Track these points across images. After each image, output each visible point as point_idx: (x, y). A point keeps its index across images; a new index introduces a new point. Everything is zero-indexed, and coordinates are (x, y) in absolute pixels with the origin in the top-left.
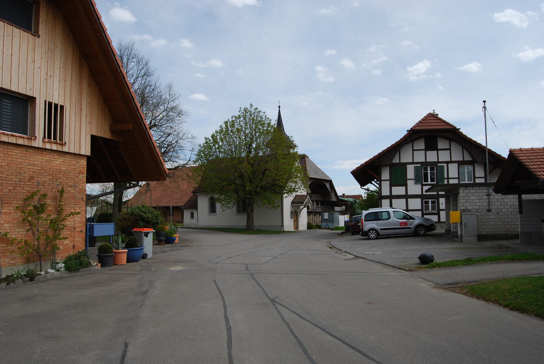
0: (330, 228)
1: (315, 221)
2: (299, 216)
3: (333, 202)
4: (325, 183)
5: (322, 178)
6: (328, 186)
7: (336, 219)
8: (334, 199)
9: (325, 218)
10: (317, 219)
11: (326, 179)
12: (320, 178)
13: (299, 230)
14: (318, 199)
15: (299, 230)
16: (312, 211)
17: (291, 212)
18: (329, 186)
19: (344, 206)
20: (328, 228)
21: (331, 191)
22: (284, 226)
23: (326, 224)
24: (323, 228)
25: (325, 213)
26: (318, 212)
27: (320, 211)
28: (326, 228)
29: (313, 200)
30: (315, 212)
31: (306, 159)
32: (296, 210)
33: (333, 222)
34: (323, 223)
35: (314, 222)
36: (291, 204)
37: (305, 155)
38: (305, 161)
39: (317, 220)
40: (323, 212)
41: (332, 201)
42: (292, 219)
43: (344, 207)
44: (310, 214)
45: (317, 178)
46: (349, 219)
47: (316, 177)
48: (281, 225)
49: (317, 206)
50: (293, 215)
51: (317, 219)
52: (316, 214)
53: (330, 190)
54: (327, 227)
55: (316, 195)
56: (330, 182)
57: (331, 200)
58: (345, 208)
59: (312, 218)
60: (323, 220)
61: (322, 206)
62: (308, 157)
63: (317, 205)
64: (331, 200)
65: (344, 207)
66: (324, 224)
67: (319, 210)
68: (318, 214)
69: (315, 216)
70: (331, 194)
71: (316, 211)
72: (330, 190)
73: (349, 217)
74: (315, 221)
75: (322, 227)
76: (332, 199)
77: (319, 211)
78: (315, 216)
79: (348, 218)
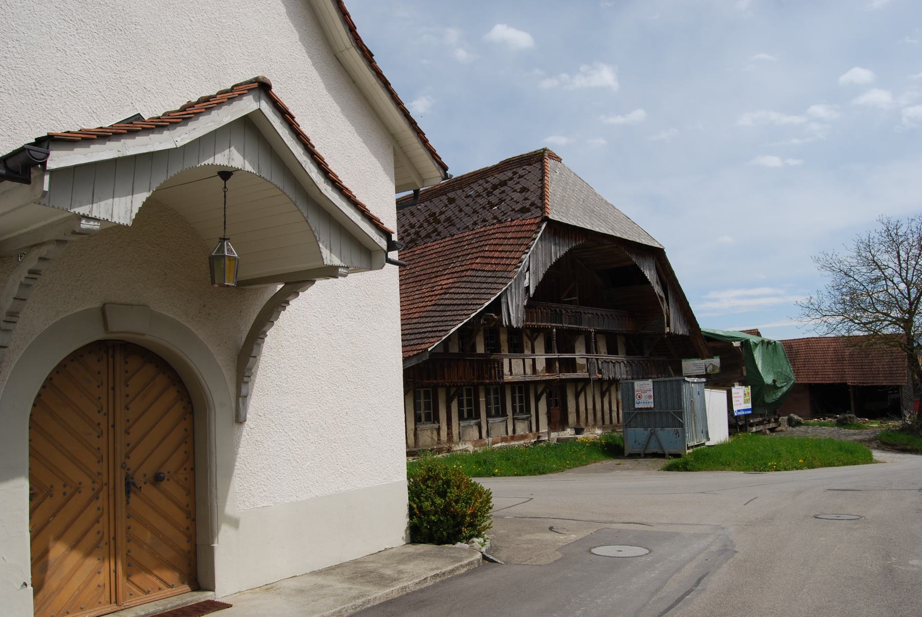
0: (667, 452)
1: (607, 417)
2: (220, 418)
3: (673, 337)
4: (634, 259)
5: (618, 235)
6: (650, 274)
7: (693, 410)
8: (676, 327)
9: (640, 406)
10: (614, 408)
11: (638, 241)
12: (611, 233)
14: (614, 327)
16: (586, 375)
18: (654, 272)
19: (716, 355)
20: (655, 455)
21: (662, 294)
23: (647, 433)
24: (633, 456)
25: (638, 385)
26: (614, 382)
27: (625, 376)
28: (647, 456)
29: (590, 332)
30: (600, 381)
31: (550, 163)
33: (682, 425)
35: (600, 422)
39: (614, 414)
41: (668, 333)
43: (716, 361)
44: (584, 389)
45: (597, 230)
46: (749, 406)
47: (589, 227)
49: (613, 358)
51: (614, 408)
52: (608, 390)
53: (658, 289)
54: (653, 448)
55: (600, 311)
56: (657, 255)
57: (667, 330)
58: (718, 365)
59: (590, 406)
60: (634, 416)
61: (631, 358)
63: (612, 350)
64: (667, 330)
65: (716, 361)
66: (636, 436)
67: (620, 372)
68: (617, 390)
69: (602, 396)
70: (664, 307)
71: (606, 377)
72: (658, 289)
73: (749, 397)
74: (607, 417)
75: (626, 453)
76: (669, 325)
78: (602, 396)
79: (746, 401)
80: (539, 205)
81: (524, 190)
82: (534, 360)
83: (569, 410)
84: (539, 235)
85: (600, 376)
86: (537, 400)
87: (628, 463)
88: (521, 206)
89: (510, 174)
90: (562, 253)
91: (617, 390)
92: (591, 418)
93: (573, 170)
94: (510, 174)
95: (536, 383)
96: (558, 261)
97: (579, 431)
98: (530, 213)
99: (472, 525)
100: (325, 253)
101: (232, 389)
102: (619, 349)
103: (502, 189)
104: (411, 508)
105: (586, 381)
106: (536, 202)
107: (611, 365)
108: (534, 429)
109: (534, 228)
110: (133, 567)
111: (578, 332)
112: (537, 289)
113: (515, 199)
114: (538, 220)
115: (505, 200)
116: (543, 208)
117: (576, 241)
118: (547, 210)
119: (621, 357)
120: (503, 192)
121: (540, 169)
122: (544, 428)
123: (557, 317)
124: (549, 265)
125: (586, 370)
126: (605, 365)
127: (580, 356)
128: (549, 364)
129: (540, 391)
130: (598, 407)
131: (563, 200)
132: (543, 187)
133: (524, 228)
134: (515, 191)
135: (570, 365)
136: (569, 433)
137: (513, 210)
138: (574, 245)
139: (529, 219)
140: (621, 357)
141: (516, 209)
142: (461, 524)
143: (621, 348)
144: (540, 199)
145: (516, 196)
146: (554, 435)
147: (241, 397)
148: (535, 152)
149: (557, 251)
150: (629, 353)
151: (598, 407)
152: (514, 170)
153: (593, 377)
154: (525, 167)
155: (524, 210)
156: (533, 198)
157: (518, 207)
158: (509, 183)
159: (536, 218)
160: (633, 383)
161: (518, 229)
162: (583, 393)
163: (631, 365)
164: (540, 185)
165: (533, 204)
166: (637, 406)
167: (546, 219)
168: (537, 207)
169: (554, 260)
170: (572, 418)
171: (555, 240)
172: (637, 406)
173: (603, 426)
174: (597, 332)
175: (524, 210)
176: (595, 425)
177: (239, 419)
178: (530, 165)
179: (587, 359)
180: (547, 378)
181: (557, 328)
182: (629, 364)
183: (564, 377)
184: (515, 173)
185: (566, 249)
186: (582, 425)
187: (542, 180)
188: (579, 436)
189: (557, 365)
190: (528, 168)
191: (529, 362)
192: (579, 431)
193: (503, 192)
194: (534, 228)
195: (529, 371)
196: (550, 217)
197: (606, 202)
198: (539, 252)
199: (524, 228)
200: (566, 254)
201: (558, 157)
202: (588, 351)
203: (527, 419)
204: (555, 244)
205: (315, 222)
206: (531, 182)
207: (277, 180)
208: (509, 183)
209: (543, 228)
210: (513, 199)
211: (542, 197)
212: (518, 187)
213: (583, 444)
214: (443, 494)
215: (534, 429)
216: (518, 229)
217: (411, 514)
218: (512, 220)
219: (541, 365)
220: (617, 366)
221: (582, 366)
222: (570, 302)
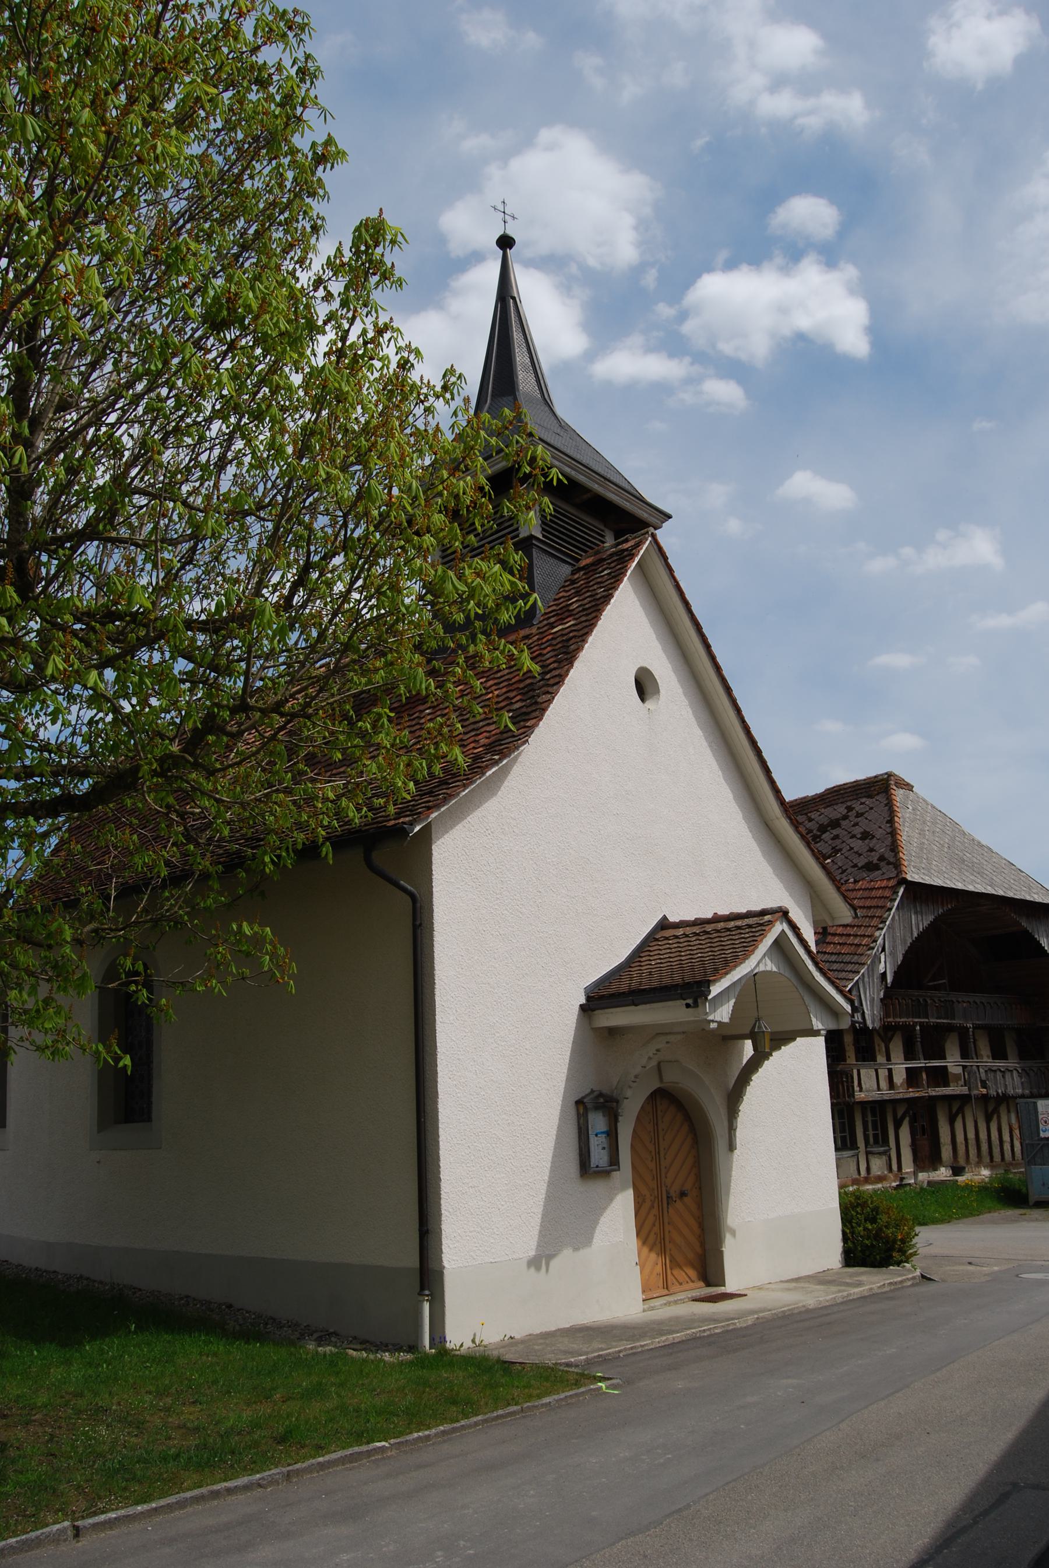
1: (996, 1151)
2: (721, 1144)
5: (1001, 893)
10: (1006, 1137)
11: (1028, 898)
12: (990, 890)
13: (730, 1287)
15: (730, 1287)
16: (965, 1090)
17: (579, 1103)
22: (440, 1274)
26: (1004, 1099)
27: (1020, 1091)
29: (967, 1029)
30: (985, 1098)
31: (898, 795)
32: (672, 1077)
34: (1036, 1169)
35: (987, 1159)
36: (586, 1009)
37: (889, 775)
38: (890, 805)
39: (1007, 1147)
40: (1032, 1096)
42: (598, 1187)
44: (961, 1110)
45: (971, 888)
47: (960, 886)
48: (412, 1261)
49: (1000, 1064)
50: (612, 1134)
51: (1006, 1137)
52: (996, 1111)
59: (971, 1135)
62: (909, 787)
63: (999, 1054)
67: (1014, 1085)
68: (1009, 1112)
69: (988, 1121)
71: (993, 1093)
74: (996, 1151)
75: (1032, 1199)
77: (1011, 1092)
78: (988, 1121)
80: (892, 860)
81: (866, 836)
82: (890, 1071)
83: (942, 1140)
84: (896, 904)
85: (984, 1091)
86: (898, 1126)
87: (1036, 1213)
88: (866, 861)
89: (842, 809)
90: (926, 924)
91: (1009, 1112)
92: (973, 1152)
93: (930, 801)
94: (842, 809)
95: (894, 1102)
96: (921, 936)
97: (957, 1171)
98: (879, 872)
99: (902, 1251)
100: (814, 1020)
101: (726, 1124)
102: (1009, 1051)
103: (835, 832)
104: (844, 1233)
105: (965, 1099)
106: (886, 856)
107: (999, 1075)
108: (895, 1167)
109: (887, 893)
110: (675, 1264)
111: (950, 1028)
112: (896, 974)
113: (855, 849)
114: (892, 883)
115: (840, 850)
116: (897, 865)
117: (943, 905)
118: (904, 868)
119: (1012, 1063)
120: (836, 837)
121: (886, 805)
122: (908, 1167)
123: (920, 1009)
124: (909, 941)
125: (962, 1082)
126: (991, 1075)
127: (953, 1062)
128: (912, 1076)
129: (900, 1114)
130: (983, 1136)
131: (921, 849)
132: (893, 833)
133: (874, 893)
134: (853, 836)
135: (940, 1076)
136: (943, 1173)
137: (855, 866)
138: (941, 911)
139: (880, 880)
140: (1012, 1063)
141: (860, 865)
142: (891, 1249)
143: (1011, 1049)
144: (892, 850)
145: (857, 844)
146: (922, 1176)
147: (732, 1129)
148: (876, 777)
149: (920, 922)
150: (1022, 1056)
151: (983, 1136)
152: (849, 804)
153: (975, 1092)
154: (863, 800)
155: (871, 867)
156: (882, 849)
157: (861, 862)
158: (844, 823)
159: (889, 879)
160: (1035, 1103)
161: (866, 894)
162: (960, 1116)
163: (1028, 1074)
164: (889, 830)
165: (882, 858)
166: (1042, 1135)
167: (904, 881)
168: (889, 863)
169: (915, 935)
170: (946, 1153)
171: (915, 907)
172: (1042, 1135)
173: (992, 1165)
174: (976, 1027)
175: (871, 867)
176: (979, 1163)
177: (731, 1147)
178: (870, 797)
179: (964, 1067)
180: (912, 1095)
181: (921, 1024)
182: (1025, 1072)
183: (934, 1094)
184: (850, 809)
185: (931, 918)
186: (962, 1162)
187: (891, 821)
188: (960, 1178)
189: (924, 1076)
190: (868, 801)
191: (883, 1073)
192: (957, 1171)
193: (836, 837)
194: (887, 893)
195: (884, 1084)
196: (909, 878)
197: (979, 843)
198: (897, 924)
199: (874, 893)
200: (931, 924)
201: (908, 784)
202: (965, 1055)
203: (884, 1153)
204: (916, 913)
205: (808, 999)
206: (873, 822)
207: (787, 973)
208: (844, 823)
209: (900, 894)
210: (852, 848)
211: (894, 847)
212: (857, 831)
213: (967, 1187)
214: (873, 1220)
215: (895, 1167)
216: (866, 894)
217: (845, 1238)
218: (855, 882)
219: (900, 1077)
220: (1008, 1075)
221: (957, 1077)
222: (936, 988)
